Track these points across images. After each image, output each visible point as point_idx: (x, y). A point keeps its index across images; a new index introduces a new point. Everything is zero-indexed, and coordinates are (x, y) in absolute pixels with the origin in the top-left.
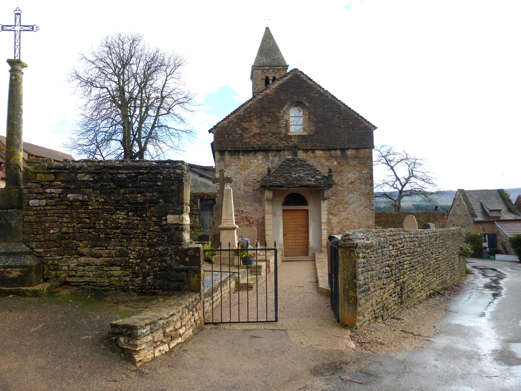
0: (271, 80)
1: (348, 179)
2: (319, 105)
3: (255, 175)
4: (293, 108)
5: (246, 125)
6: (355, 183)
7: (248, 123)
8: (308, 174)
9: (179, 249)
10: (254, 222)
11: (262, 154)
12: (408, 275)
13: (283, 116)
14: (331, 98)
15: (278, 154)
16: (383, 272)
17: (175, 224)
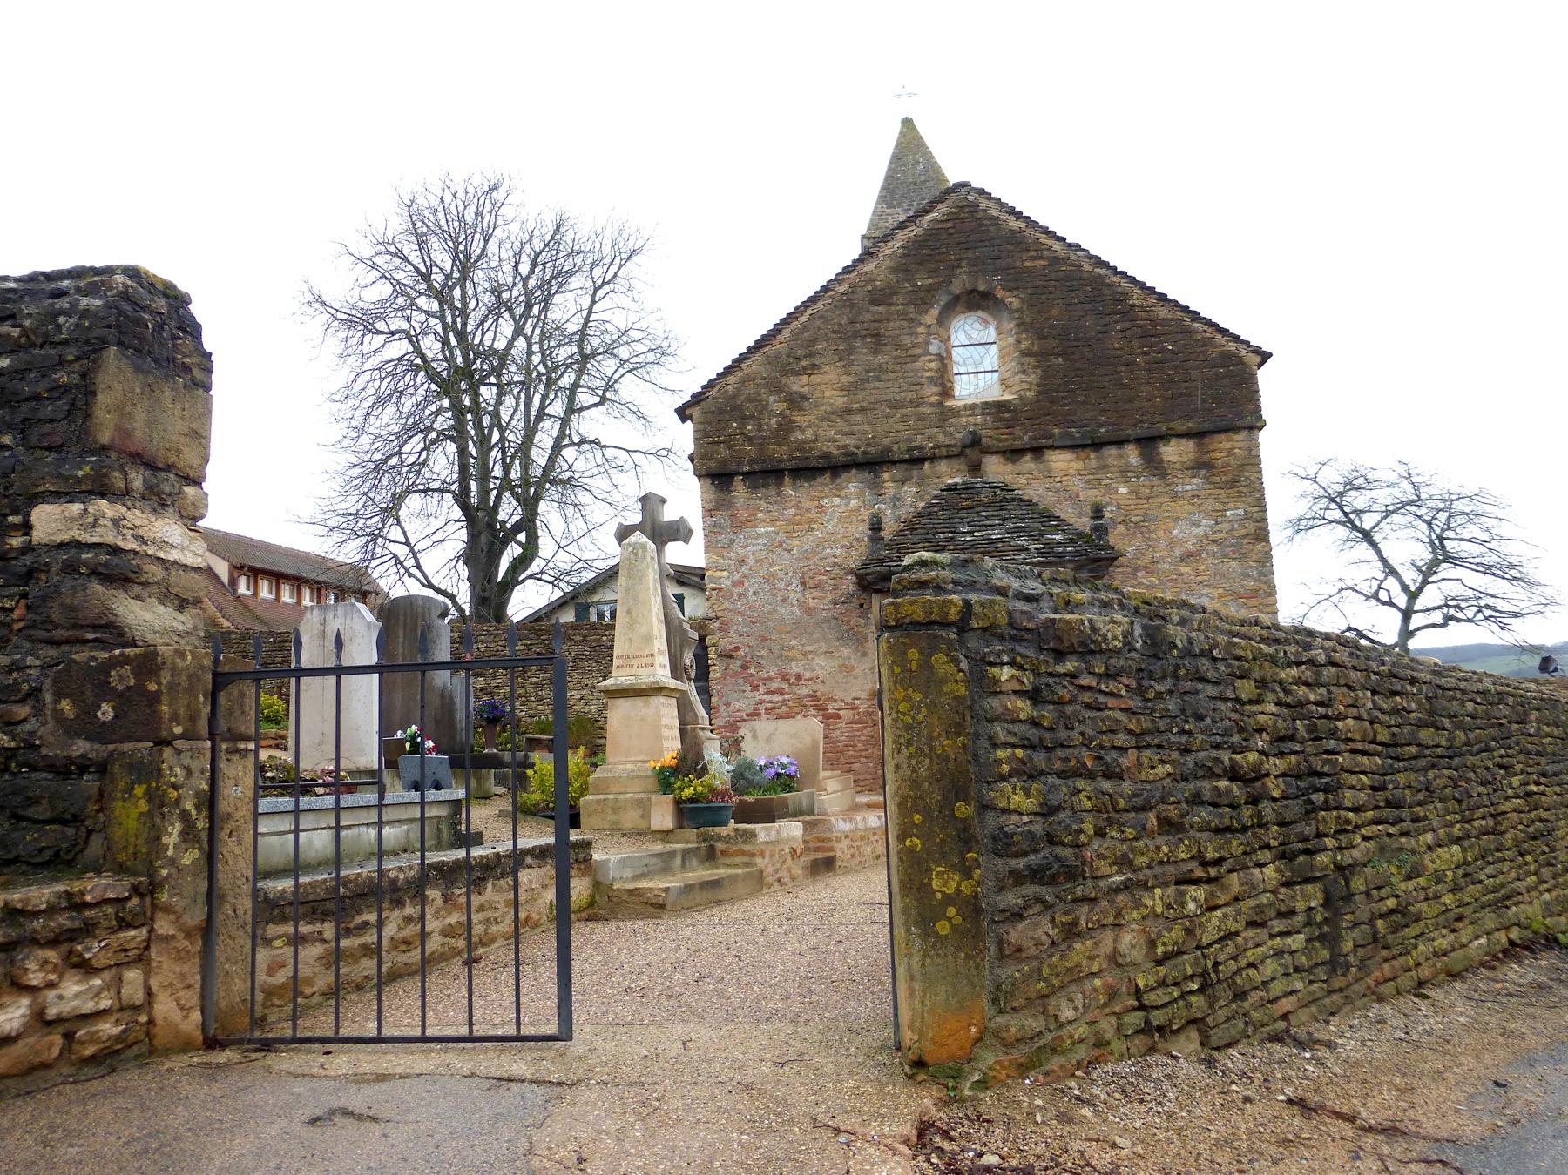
1: (1172, 544)
2: (1052, 296)
3: (839, 551)
4: (963, 316)
5: (798, 384)
6: (1200, 555)
7: (806, 377)
8: (1017, 530)
9: (73, 661)
10: (841, 713)
11: (860, 476)
12: (1366, 838)
13: (927, 343)
14: (1091, 269)
15: (915, 473)
16: (1196, 800)
17: (62, 545)
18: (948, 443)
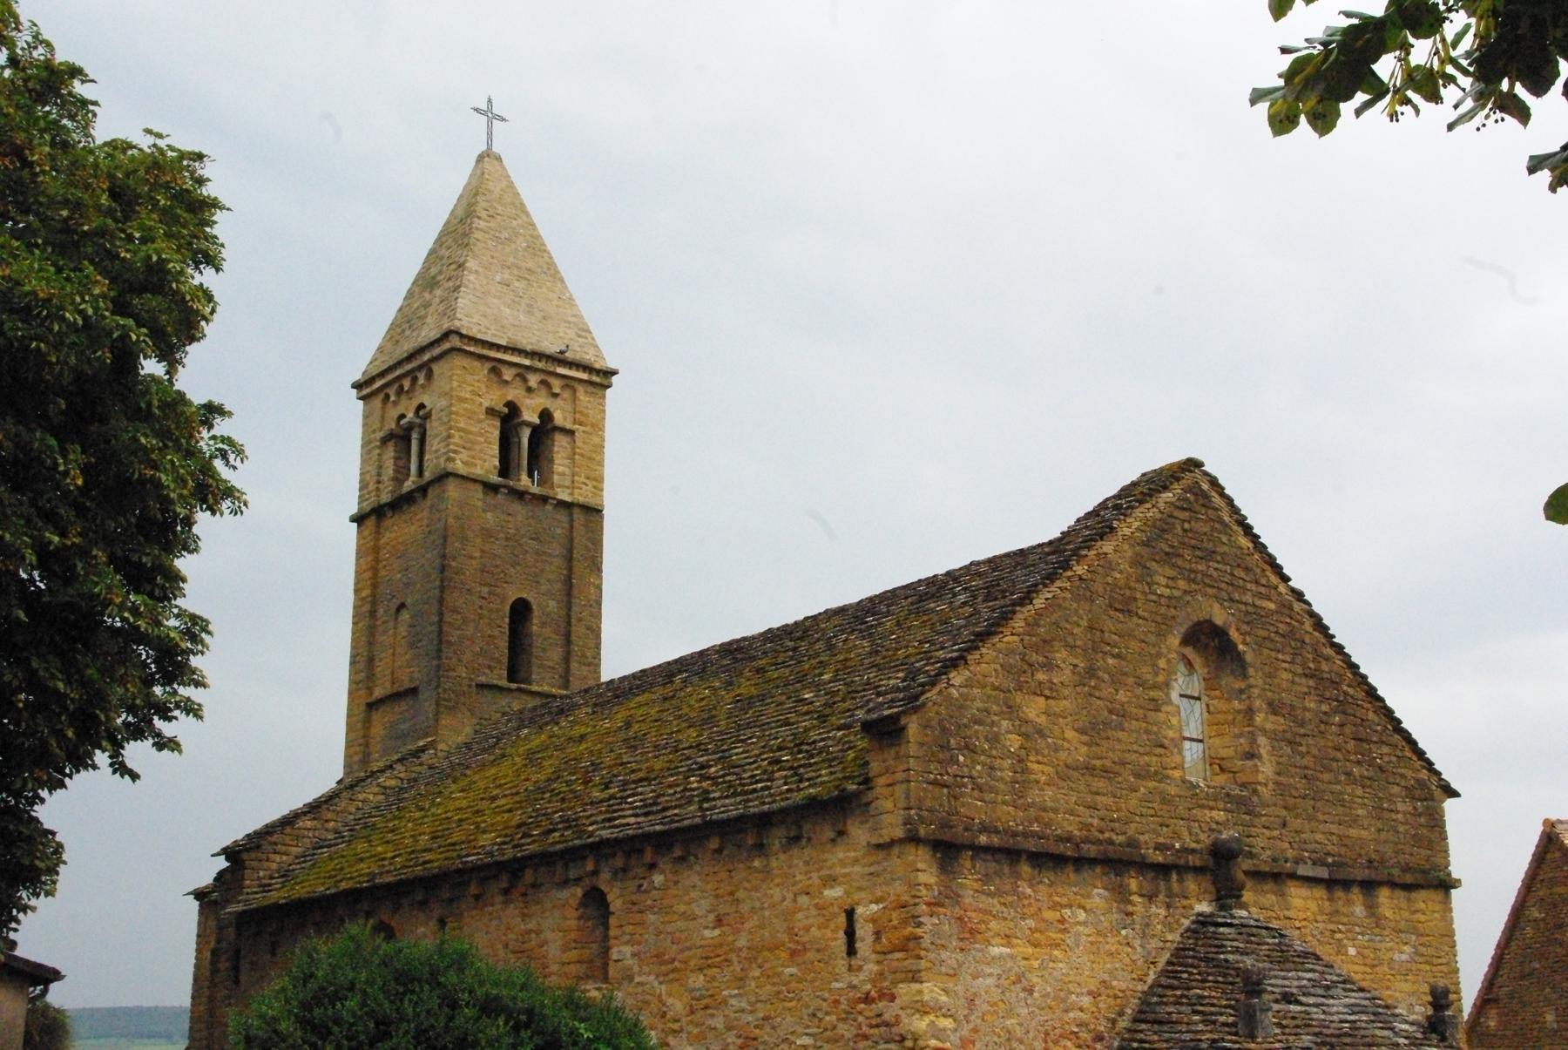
0: (528, 424)
18: (1193, 845)
